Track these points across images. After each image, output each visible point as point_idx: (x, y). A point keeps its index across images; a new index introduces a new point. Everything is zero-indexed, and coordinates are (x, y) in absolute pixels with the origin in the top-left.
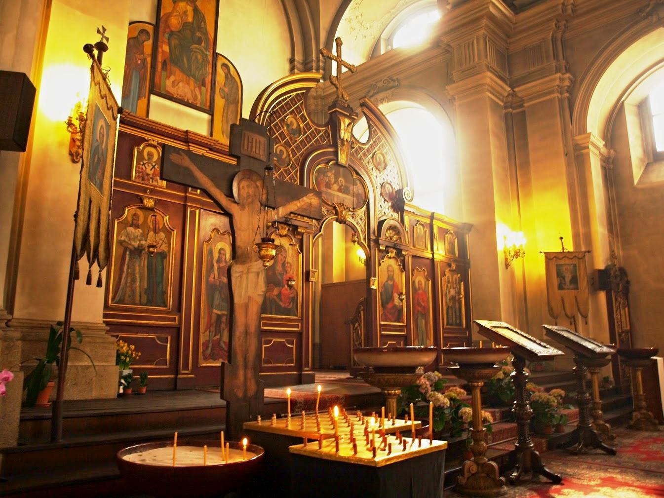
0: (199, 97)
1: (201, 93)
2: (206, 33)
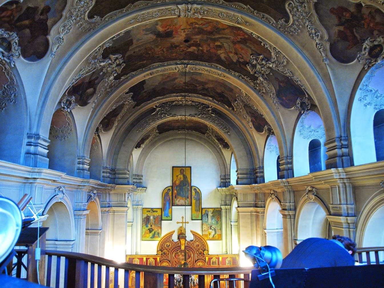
0: (187, 202)
2: (188, 181)
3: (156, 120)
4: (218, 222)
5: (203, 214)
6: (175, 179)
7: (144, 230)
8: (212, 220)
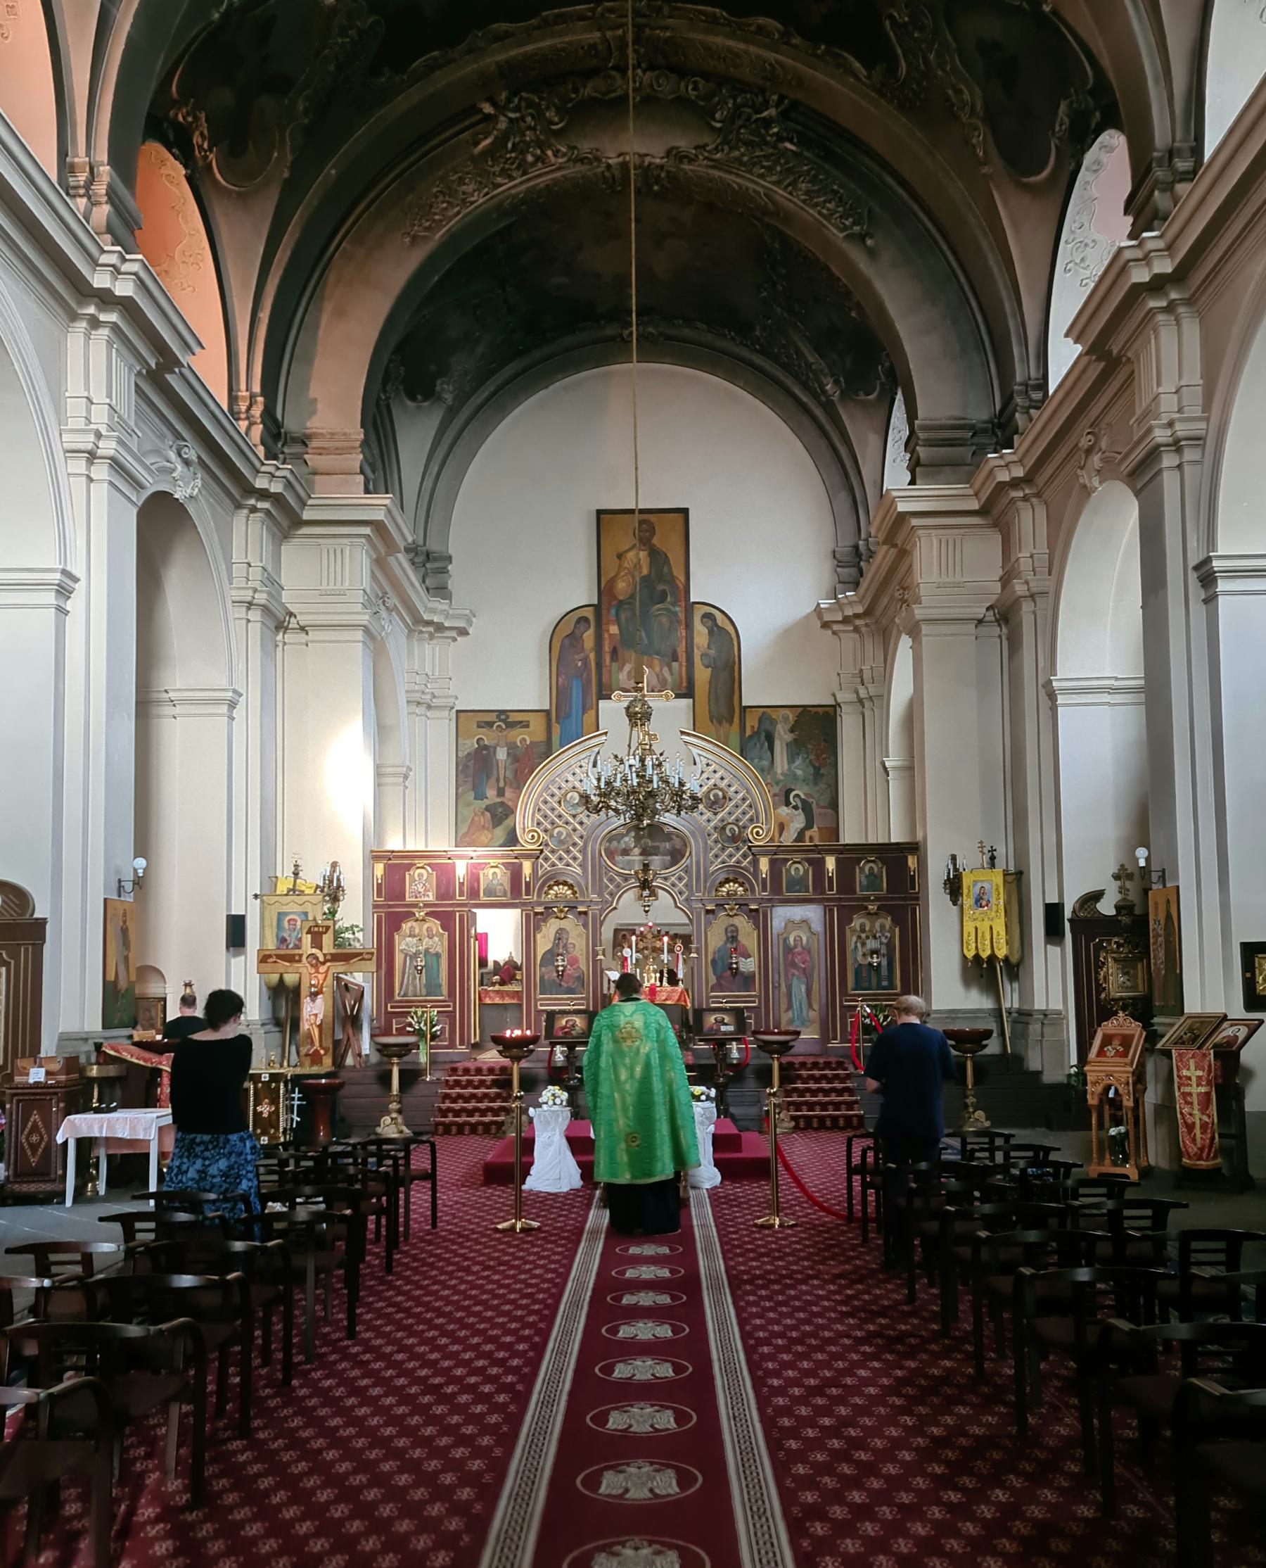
1: (672, 674)
2: (672, 580)
3: (499, 180)
4: (822, 772)
5: (748, 733)
6: (610, 571)
7: (468, 813)
8: (791, 760)
